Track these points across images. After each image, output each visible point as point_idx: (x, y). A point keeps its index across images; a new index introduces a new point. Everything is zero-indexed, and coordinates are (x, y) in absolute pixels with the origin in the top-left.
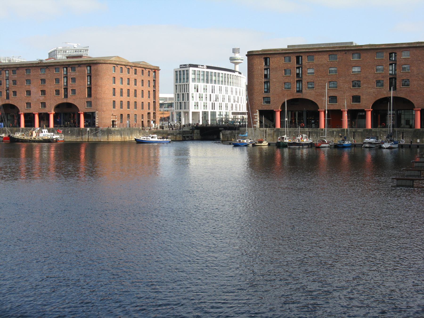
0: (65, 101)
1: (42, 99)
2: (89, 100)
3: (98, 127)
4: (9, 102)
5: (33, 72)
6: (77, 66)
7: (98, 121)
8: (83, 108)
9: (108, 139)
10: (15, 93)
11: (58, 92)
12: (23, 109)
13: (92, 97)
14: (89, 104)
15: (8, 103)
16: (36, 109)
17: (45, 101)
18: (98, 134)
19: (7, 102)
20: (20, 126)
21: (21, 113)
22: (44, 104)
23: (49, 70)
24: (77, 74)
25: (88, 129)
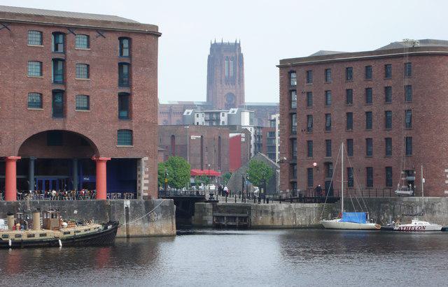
0: (58, 125)
3: (149, 197)
6: (96, 34)
7: (147, 182)
8: (108, 149)
13: (135, 121)
14: (126, 136)
23: (12, 35)
24: (94, 54)
25: (127, 203)
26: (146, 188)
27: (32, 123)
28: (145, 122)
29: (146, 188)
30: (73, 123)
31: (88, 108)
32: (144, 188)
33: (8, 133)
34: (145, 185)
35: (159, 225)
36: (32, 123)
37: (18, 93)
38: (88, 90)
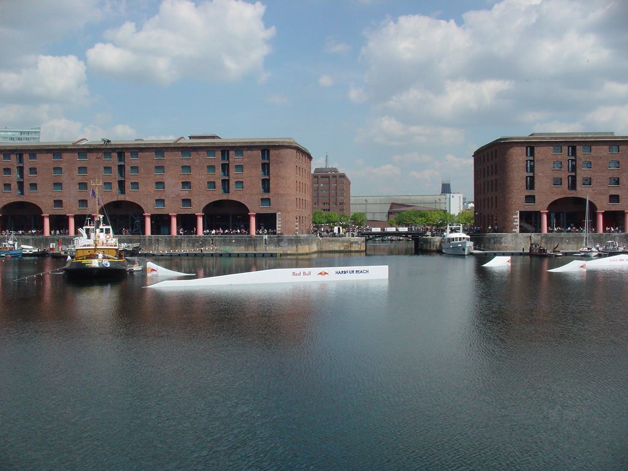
1: (185, 193)
2: (266, 196)
3: (281, 234)
5: (168, 155)
7: (280, 225)
8: (255, 208)
9: (297, 251)
10: (135, 185)
11: (212, 184)
12: (150, 208)
16: (173, 209)
17: (189, 198)
18: (281, 244)
20: (144, 233)
21: (146, 214)
22: (187, 202)
24: (246, 160)
25: (266, 237)
26: (280, 229)
27: (209, 196)
28: (279, 194)
29: (280, 229)
30: (234, 196)
31: (243, 188)
32: (277, 229)
34: (279, 227)
35: (286, 249)
36: (209, 196)
37: (202, 182)
38: (242, 178)
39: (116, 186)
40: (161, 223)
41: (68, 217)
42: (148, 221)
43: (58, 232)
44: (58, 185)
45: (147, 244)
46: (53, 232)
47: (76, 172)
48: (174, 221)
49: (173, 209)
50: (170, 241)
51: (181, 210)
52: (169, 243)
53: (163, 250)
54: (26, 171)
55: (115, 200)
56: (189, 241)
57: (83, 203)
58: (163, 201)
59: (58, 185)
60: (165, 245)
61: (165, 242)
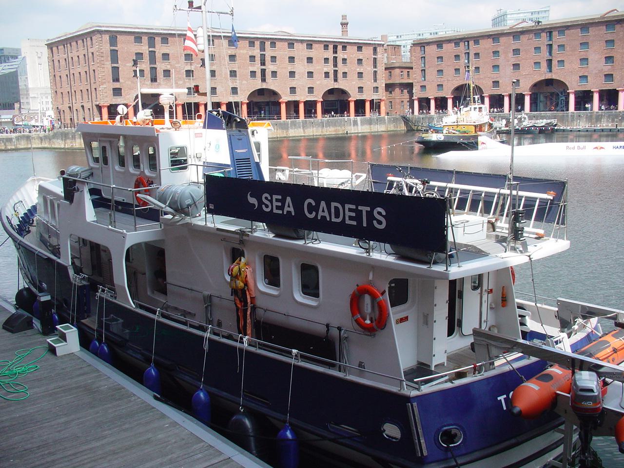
4: (552, 76)
12: (574, 86)
15: (550, 78)
19: (549, 76)
20: (568, 110)
33: (618, 77)
39: (544, 65)
40: (584, 98)
41: (592, 92)
42: (572, 99)
43: (495, 110)
44: (496, 67)
45: (570, 120)
46: (492, 110)
47: (511, 54)
48: (596, 97)
49: (595, 85)
50: (591, 116)
51: (603, 85)
52: (589, 119)
53: (583, 125)
54: (472, 56)
55: (543, 79)
56: (609, 117)
57: (517, 83)
58: (586, 77)
59: (496, 67)
60: (586, 121)
61: (586, 118)
